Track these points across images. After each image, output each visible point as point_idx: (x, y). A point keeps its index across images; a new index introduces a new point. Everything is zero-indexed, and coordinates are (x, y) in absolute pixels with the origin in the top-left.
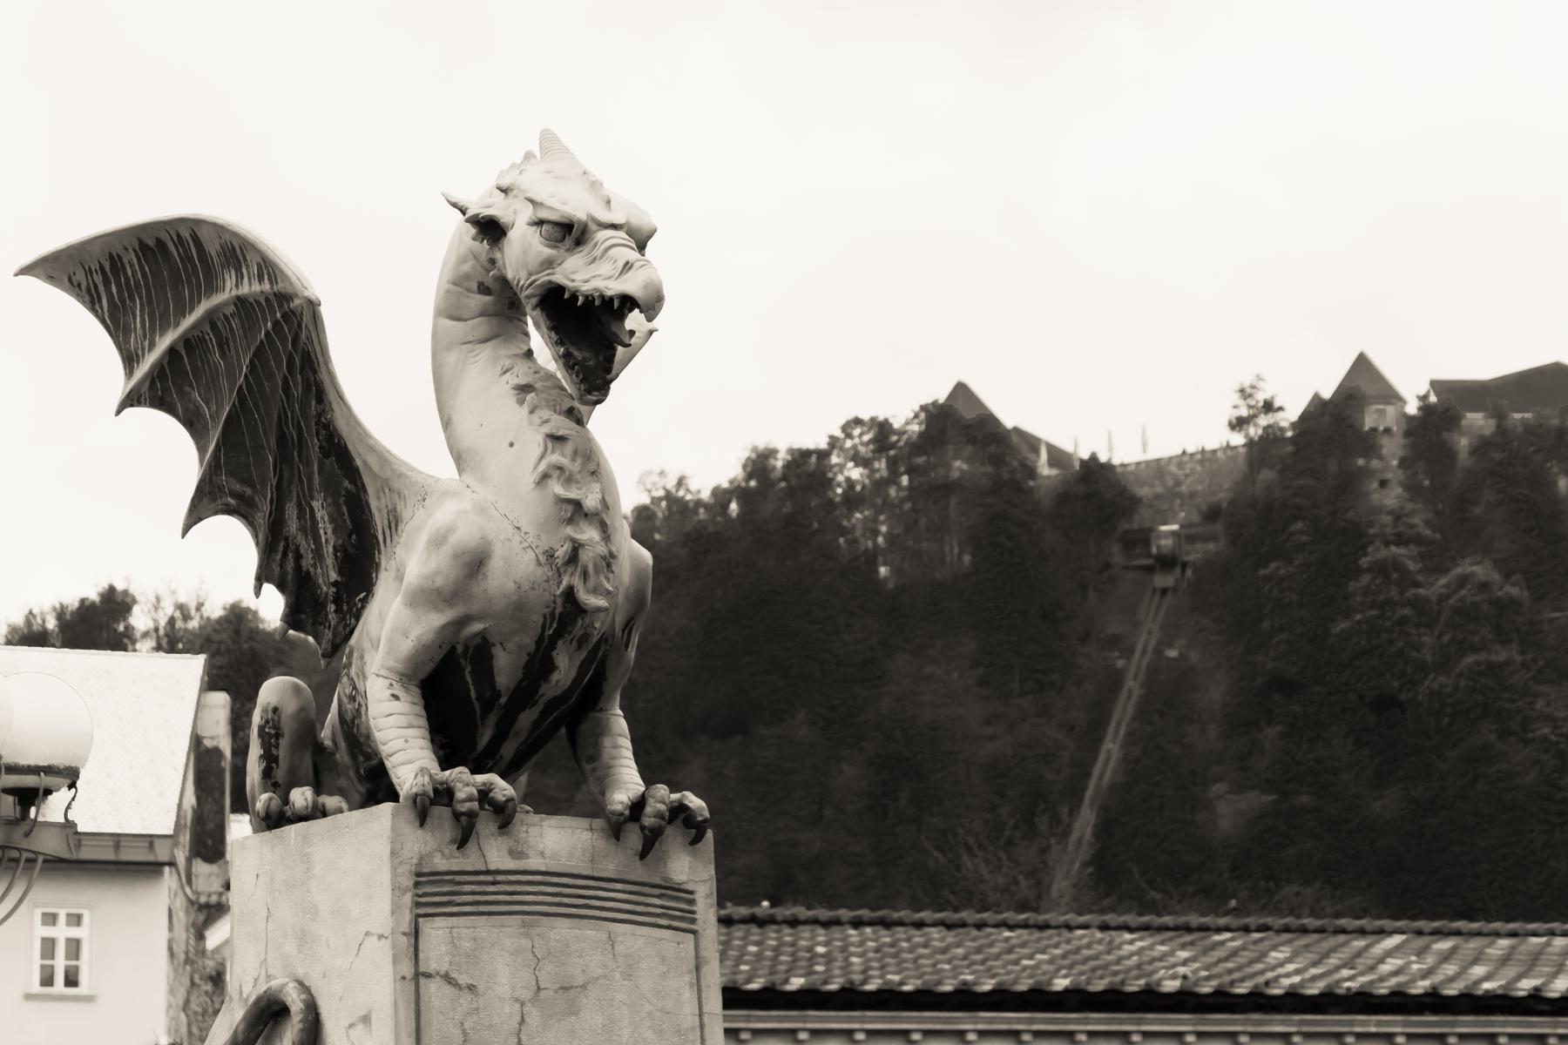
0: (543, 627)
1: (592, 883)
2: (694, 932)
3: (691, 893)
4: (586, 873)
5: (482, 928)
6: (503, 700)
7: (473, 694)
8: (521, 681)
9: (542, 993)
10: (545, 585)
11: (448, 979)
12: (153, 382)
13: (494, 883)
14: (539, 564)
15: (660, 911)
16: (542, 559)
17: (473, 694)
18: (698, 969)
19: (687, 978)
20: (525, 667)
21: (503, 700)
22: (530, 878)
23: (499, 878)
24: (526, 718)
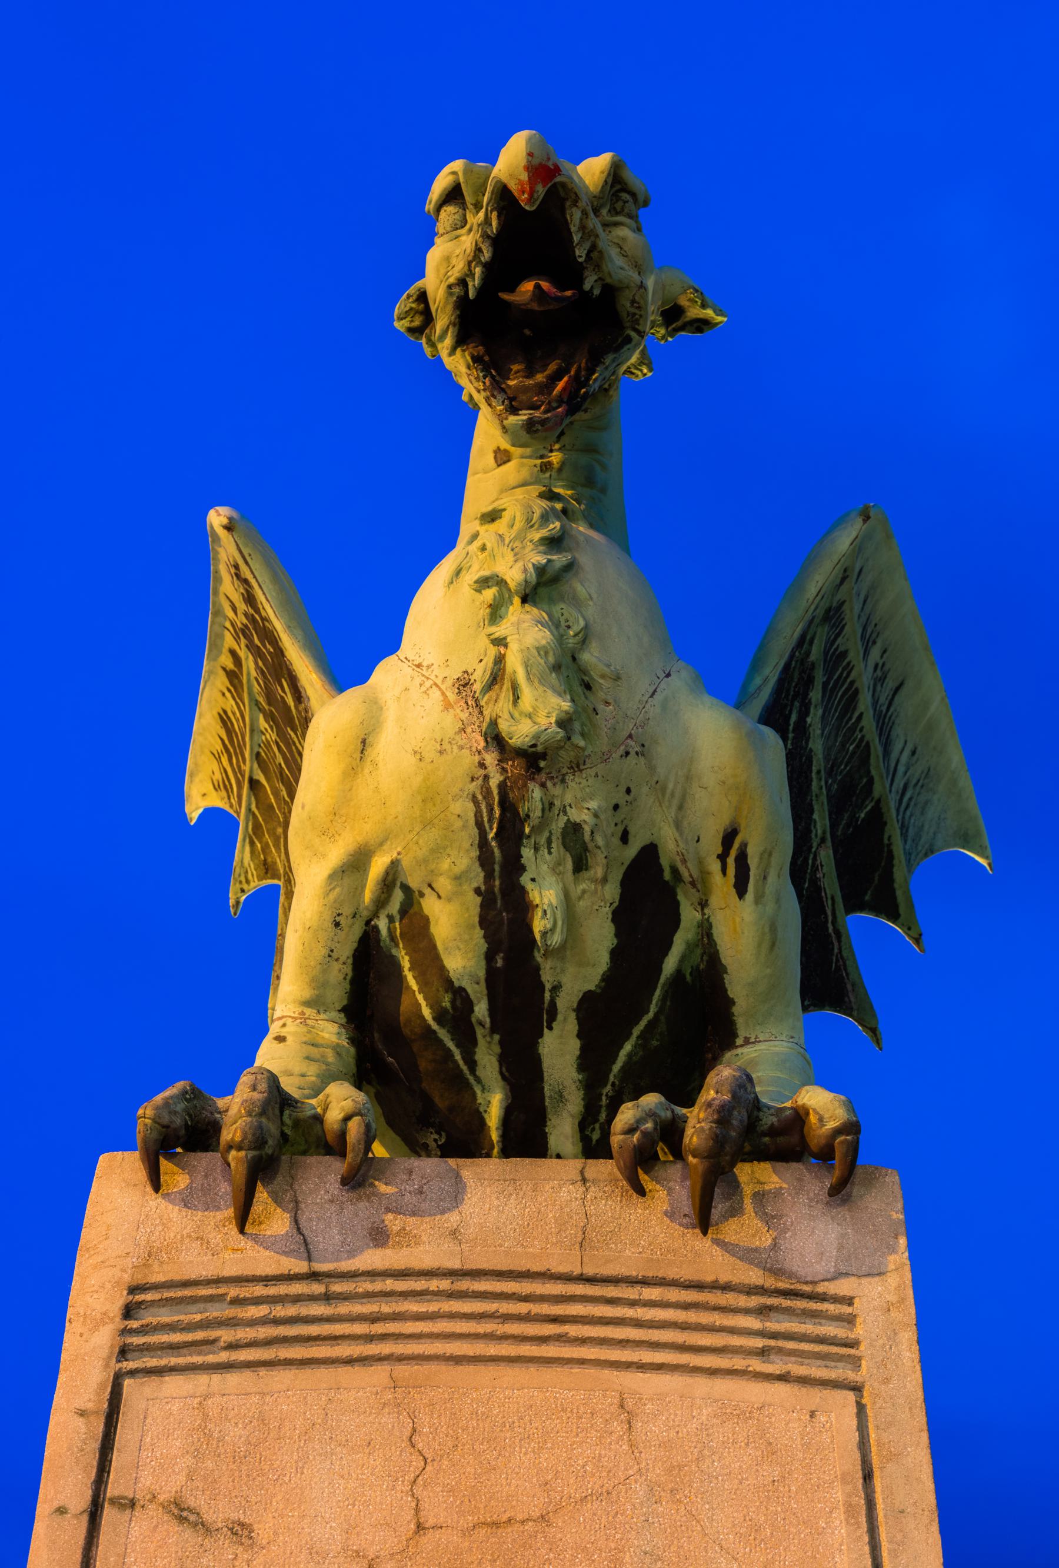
0: (479, 824)
1: (579, 1289)
2: (857, 1389)
3: (849, 1301)
4: (563, 1269)
5: (289, 1393)
6: (481, 1010)
7: (426, 1012)
8: (489, 957)
9: (428, 1540)
10: (461, 740)
11: (181, 1512)
12: (252, 844)
13: (327, 1298)
14: (448, 706)
15: (759, 1343)
16: (452, 696)
17: (426, 1012)
18: (868, 1476)
19: (838, 1494)
20: (483, 922)
21: (481, 1010)
22: (420, 1285)
23: (337, 1287)
24: (559, 1051)
